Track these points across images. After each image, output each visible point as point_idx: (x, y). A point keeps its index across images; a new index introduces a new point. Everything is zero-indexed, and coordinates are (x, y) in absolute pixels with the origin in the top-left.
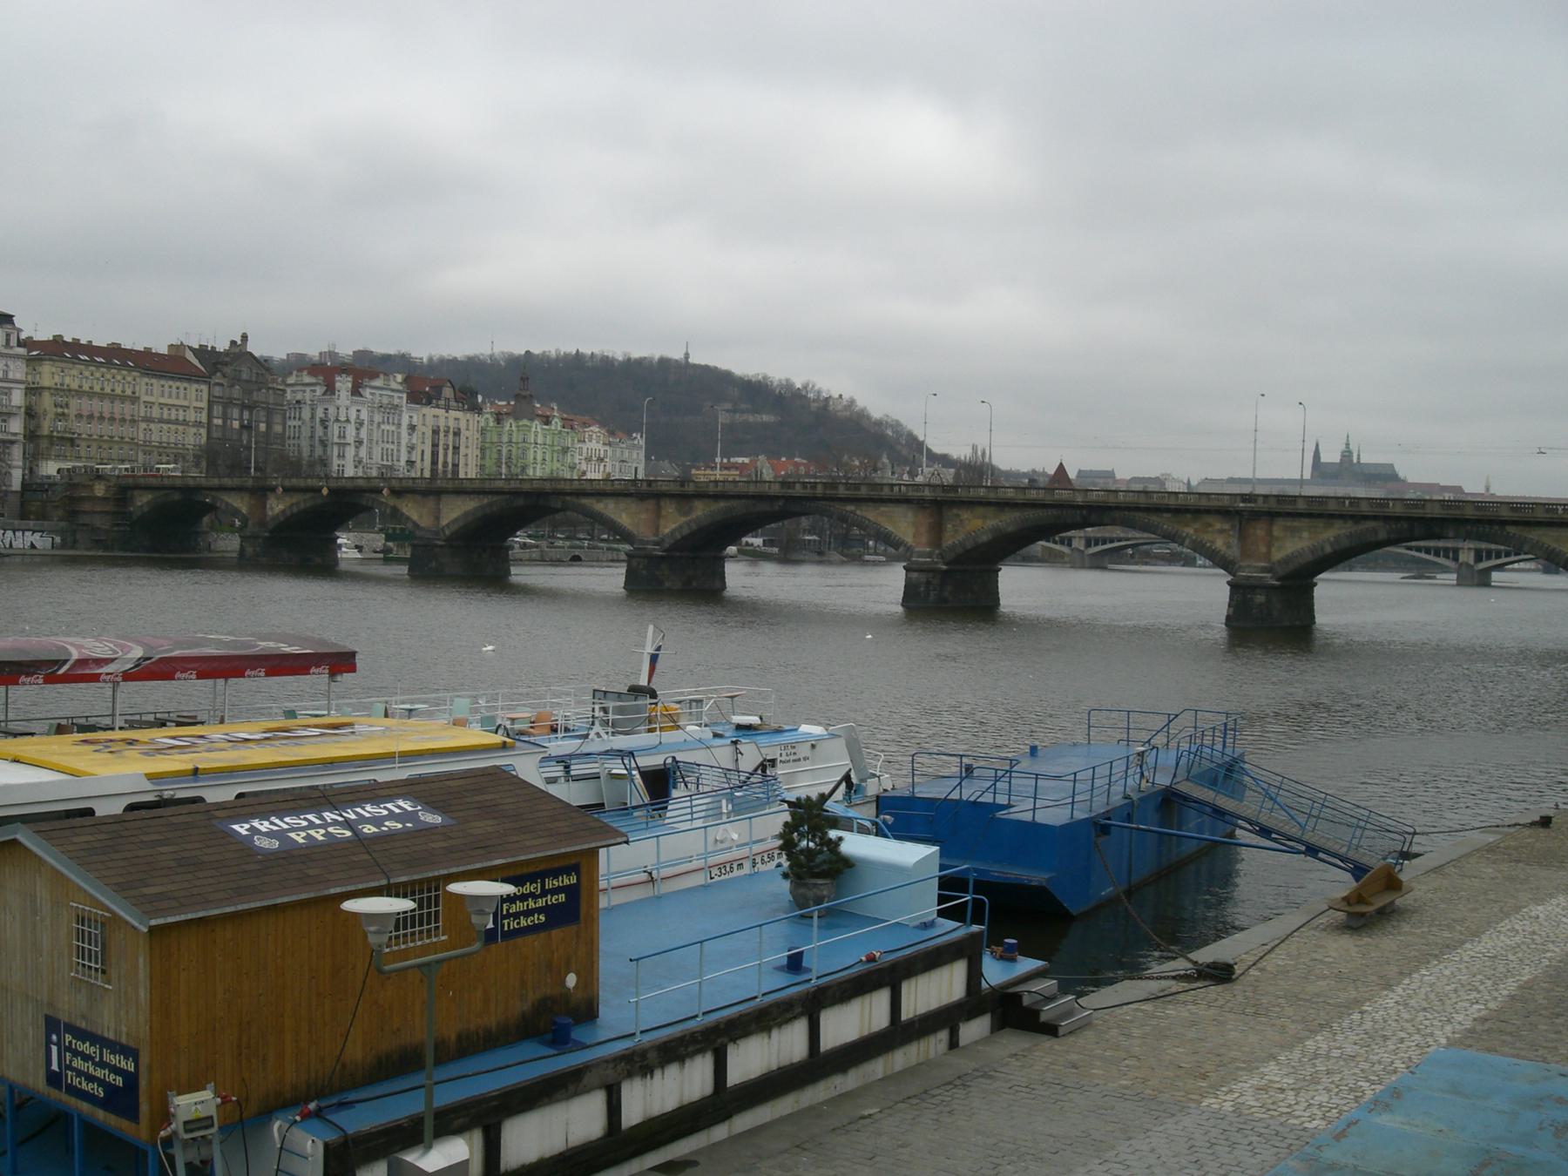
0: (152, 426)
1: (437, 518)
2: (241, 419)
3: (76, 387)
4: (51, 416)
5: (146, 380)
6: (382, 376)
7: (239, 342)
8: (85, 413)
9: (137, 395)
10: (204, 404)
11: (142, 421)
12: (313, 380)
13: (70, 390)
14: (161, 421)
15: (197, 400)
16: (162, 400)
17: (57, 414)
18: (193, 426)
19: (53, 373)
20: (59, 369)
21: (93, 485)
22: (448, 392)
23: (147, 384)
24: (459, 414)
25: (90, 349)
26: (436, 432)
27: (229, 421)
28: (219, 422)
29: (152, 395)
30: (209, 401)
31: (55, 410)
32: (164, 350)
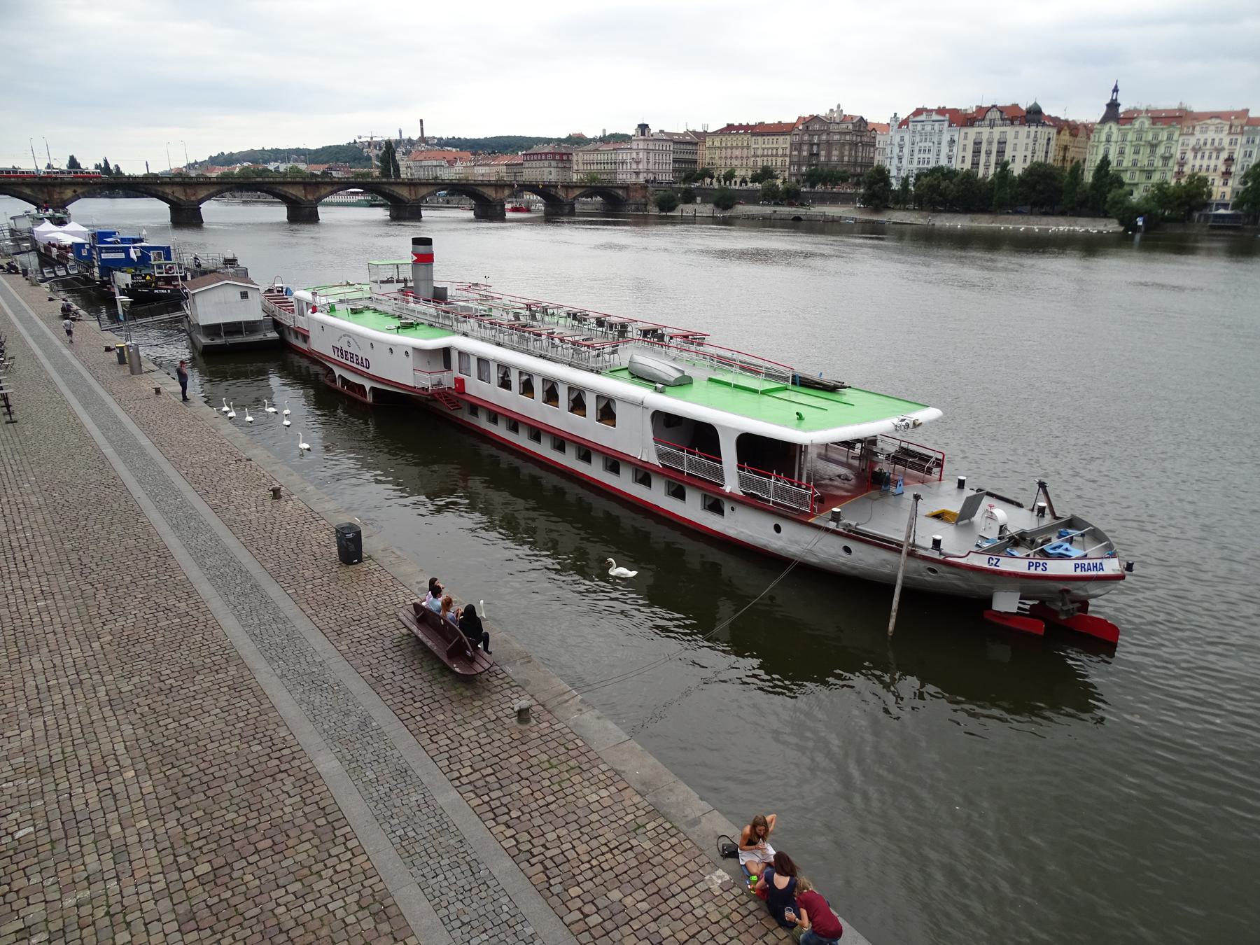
5: (754, 138)
6: (924, 113)
10: (788, 145)
12: (942, 118)
16: (764, 146)
22: (990, 116)
24: (1004, 129)
26: (977, 144)
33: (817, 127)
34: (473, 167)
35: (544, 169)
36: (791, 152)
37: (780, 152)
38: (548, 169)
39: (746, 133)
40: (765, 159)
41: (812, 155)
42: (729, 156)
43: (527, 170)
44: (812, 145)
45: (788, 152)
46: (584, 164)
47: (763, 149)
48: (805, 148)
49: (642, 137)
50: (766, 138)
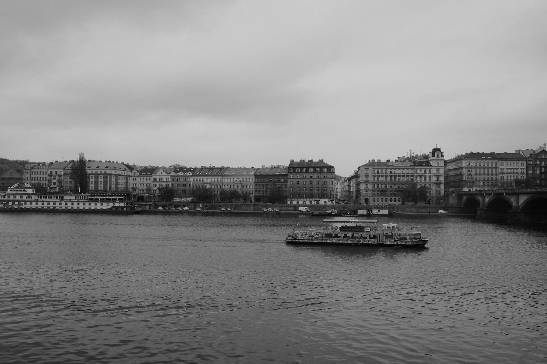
0: (504, 175)
1: (518, 203)
2: (540, 170)
3: (475, 166)
4: (466, 174)
5: (500, 162)
7: (543, 147)
8: (478, 173)
9: (497, 166)
10: (525, 167)
11: (500, 174)
13: (472, 167)
14: (507, 173)
15: (521, 166)
17: (468, 174)
18: (520, 174)
19: (466, 163)
20: (468, 162)
21: (452, 194)
23: (501, 163)
25: (483, 154)
27: (535, 172)
28: (531, 172)
29: (503, 165)
30: (526, 166)
31: (467, 173)
32: (514, 152)
33: (543, 156)
34: (192, 176)
35: (328, 180)
36: (527, 171)
37: (519, 171)
38: (331, 180)
39: (486, 159)
40: (509, 175)
41: (541, 173)
42: (490, 173)
43: (293, 180)
44: (541, 167)
45: (525, 171)
46: (374, 176)
47: (507, 169)
48: (538, 169)
49: (442, 158)
50: (509, 162)
